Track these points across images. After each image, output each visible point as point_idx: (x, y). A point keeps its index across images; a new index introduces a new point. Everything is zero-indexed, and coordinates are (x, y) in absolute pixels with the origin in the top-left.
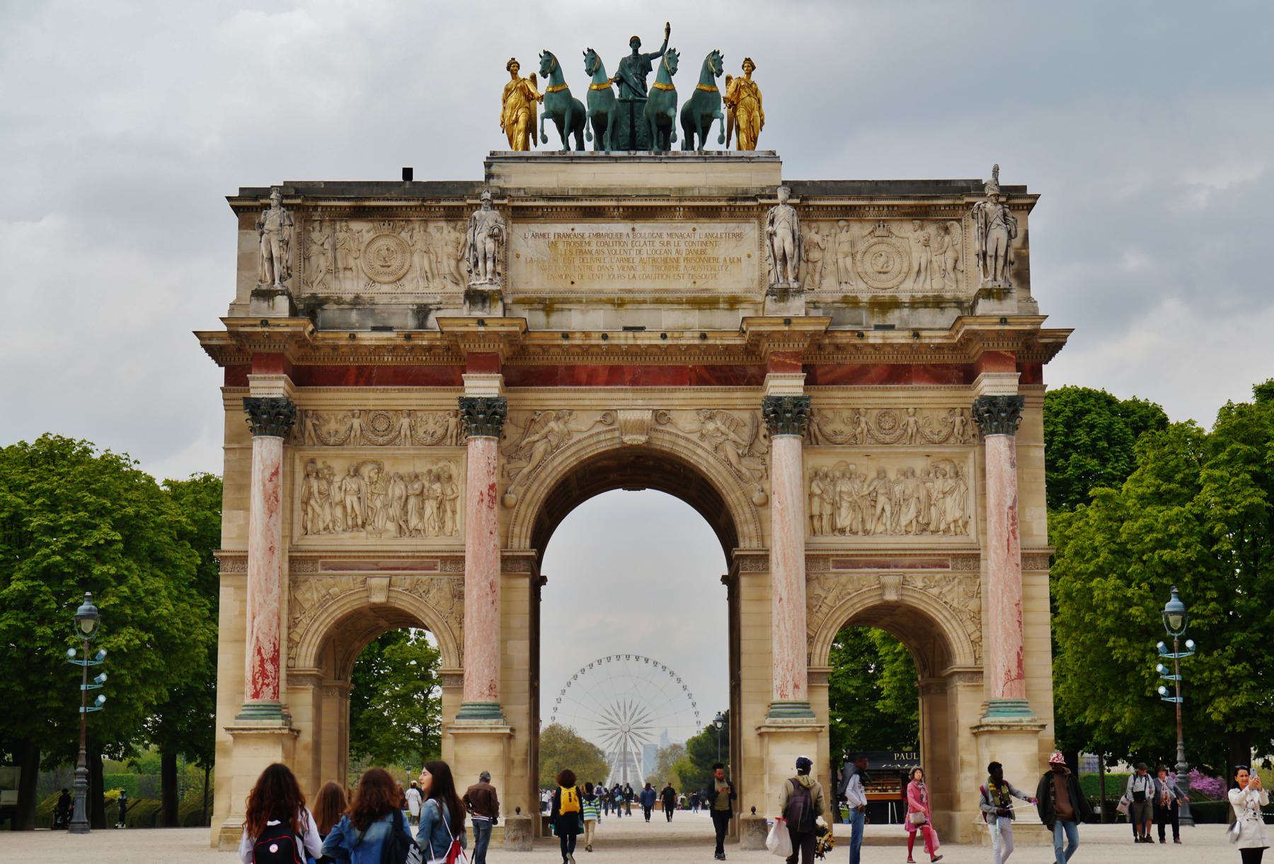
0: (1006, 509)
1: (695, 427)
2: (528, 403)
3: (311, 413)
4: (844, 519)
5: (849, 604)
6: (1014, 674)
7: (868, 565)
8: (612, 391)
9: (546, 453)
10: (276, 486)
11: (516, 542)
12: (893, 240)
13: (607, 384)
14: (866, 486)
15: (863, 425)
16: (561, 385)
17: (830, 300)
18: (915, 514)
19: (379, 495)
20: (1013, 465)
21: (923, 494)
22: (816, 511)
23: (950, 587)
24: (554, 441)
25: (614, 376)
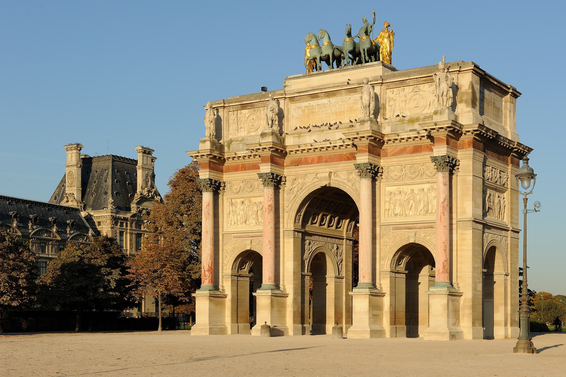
0: (440, 203)
1: (345, 178)
2: (293, 173)
3: (228, 182)
4: (398, 210)
5: (397, 244)
6: (441, 271)
7: (405, 228)
8: (318, 166)
9: (298, 191)
10: (208, 210)
11: (289, 225)
12: (421, 93)
13: (318, 163)
14: (406, 196)
15: (403, 172)
16: (303, 165)
17: (394, 121)
18: (423, 207)
19: (250, 210)
20: (445, 185)
21: (426, 199)
22: (387, 207)
23: (433, 236)
24: (300, 186)
25: (320, 160)
